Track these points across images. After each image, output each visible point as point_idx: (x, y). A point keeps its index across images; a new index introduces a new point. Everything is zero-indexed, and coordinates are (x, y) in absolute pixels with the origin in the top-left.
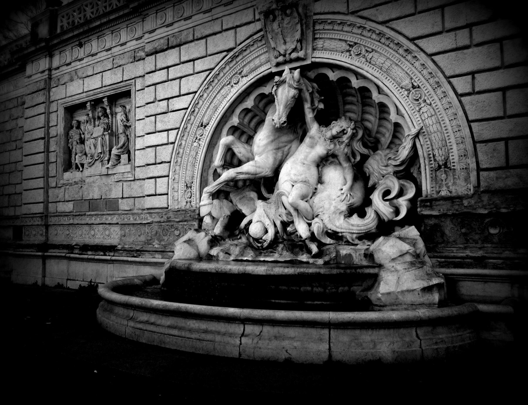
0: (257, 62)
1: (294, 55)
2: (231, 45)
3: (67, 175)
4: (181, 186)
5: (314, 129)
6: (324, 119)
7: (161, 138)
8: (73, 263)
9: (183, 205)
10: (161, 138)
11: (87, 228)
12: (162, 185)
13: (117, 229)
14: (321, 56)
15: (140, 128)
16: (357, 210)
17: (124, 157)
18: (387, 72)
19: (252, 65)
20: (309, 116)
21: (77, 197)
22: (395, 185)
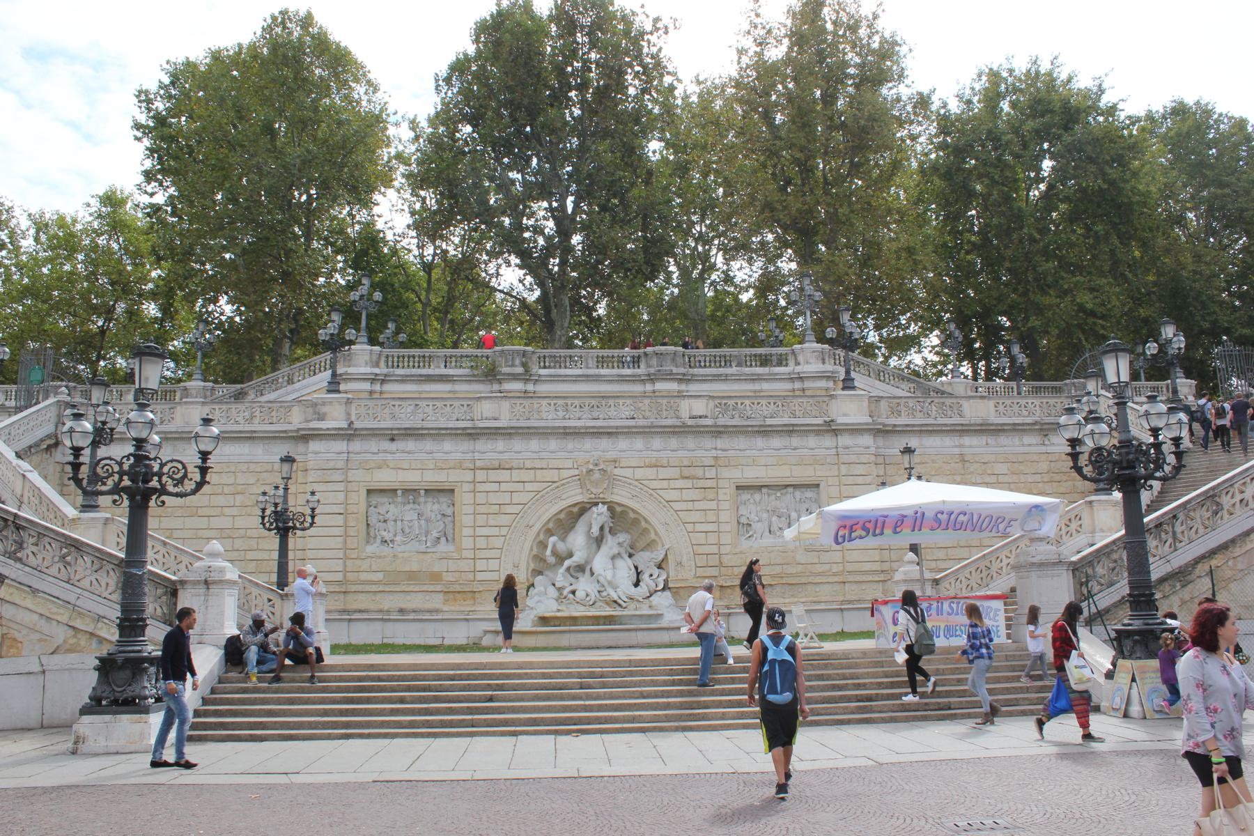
3: (370, 549)
5: (609, 537)
6: (612, 532)
7: (495, 531)
8: (390, 624)
10: (495, 531)
12: (493, 565)
13: (441, 595)
15: (467, 520)
16: (637, 585)
17: (443, 539)
20: (607, 530)
22: (656, 572)
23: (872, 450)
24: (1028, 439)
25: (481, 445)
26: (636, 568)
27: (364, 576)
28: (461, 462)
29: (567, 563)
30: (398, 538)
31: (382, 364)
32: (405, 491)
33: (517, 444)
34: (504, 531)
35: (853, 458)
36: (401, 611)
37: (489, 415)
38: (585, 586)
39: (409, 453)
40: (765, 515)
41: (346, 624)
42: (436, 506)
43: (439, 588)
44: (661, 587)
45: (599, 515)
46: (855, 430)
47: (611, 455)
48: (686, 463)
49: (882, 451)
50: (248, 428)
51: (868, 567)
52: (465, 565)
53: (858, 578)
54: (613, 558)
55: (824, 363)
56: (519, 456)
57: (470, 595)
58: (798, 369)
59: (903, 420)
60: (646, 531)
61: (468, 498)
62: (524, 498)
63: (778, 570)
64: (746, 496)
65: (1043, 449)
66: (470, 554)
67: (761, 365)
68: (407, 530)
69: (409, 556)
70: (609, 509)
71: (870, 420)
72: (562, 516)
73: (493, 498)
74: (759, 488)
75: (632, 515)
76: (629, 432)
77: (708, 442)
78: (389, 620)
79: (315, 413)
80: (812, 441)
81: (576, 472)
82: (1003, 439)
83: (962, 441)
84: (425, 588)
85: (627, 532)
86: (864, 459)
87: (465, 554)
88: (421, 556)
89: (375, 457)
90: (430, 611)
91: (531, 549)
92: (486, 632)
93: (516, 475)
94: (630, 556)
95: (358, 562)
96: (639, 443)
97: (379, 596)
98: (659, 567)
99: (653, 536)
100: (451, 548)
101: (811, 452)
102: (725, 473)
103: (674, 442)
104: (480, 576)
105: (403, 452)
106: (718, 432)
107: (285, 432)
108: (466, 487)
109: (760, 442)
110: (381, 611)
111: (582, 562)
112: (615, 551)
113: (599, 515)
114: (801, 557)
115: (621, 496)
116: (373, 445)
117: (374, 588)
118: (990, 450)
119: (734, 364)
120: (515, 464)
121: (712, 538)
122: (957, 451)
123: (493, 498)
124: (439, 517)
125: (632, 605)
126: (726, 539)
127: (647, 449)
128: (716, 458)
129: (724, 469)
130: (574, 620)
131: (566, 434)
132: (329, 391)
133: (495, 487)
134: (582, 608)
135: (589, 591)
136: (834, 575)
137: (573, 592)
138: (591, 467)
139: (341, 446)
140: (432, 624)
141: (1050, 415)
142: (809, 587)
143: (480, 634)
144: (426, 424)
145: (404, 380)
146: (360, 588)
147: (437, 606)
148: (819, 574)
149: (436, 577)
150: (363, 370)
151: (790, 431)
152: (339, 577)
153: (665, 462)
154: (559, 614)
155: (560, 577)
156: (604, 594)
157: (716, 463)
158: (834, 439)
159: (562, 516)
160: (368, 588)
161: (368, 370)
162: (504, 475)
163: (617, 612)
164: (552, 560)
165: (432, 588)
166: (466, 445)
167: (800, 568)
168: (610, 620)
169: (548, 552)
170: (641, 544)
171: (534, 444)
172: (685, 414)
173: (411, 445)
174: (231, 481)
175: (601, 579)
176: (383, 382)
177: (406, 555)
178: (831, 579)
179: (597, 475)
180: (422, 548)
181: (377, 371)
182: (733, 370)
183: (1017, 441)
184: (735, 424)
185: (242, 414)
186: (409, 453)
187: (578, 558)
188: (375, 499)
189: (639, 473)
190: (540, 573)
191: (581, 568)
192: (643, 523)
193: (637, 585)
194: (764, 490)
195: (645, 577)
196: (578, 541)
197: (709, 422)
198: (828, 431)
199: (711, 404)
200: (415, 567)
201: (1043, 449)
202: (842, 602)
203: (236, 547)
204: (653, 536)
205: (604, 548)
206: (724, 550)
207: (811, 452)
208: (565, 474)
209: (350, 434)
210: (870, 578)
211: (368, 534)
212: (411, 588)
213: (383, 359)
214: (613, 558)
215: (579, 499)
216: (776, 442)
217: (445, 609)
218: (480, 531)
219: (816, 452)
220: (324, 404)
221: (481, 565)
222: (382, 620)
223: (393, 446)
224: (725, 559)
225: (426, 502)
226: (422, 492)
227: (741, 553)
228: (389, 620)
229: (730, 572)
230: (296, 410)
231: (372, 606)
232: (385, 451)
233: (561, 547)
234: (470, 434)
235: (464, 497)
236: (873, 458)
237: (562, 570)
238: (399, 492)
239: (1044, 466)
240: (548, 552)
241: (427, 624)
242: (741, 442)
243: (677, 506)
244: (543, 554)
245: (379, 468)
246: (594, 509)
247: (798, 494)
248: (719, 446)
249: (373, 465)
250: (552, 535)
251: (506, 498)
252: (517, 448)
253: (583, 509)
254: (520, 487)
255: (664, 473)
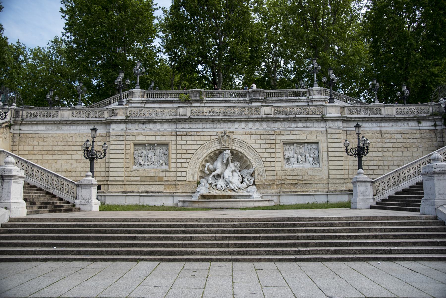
0: (216, 145)
1: (228, 146)
2: (209, 140)
3: (135, 167)
4: (190, 174)
5: (231, 163)
9: (191, 180)
11: (147, 186)
13: (163, 186)
14: (234, 148)
15: (173, 156)
16: (242, 183)
17: (164, 164)
18: (249, 154)
19: (215, 146)
20: (230, 160)
21: (142, 175)
22: (250, 178)
23: (341, 128)
24: (411, 124)
25: (179, 126)
26: (242, 176)
27: (132, 178)
28: (171, 133)
29: (213, 173)
30: (146, 163)
31: (145, 96)
32: (149, 144)
33: (194, 125)
34: (188, 160)
35: (333, 132)
36: (147, 192)
37: (182, 114)
38: (221, 183)
39: (150, 129)
40: (295, 155)
41: (125, 197)
42: (161, 151)
43: (162, 183)
44: (252, 184)
45: (227, 154)
46: (334, 120)
47: (231, 130)
48: (262, 133)
49: (345, 129)
50: (87, 119)
51: (339, 177)
52: (173, 174)
53: (334, 182)
54: (232, 172)
55: (321, 95)
56: (194, 130)
57: (174, 186)
58: (310, 97)
59: (355, 116)
60: (246, 161)
61: (174, 147)
62: (196, 147)
63: (300, 177)
64: (287, 147)
65: (418, 128)
66: (174, 170)
67: (295, 96)
68: (150, 160)
69: (151, 170)
70: (231, 152)
71: (341, 116)
72: (212, 154)
73: (184, 147)
74: (293, 144)
75: (240, 155)
76: (239, 120)
77: (272, 125)
78: (142, 196)
79: (113, 113)
80: (315, 124)
81: (217, 137)
82: (399, 124)
83: (381, 125)
84: (156, 183)
85: (239, 162)
86: (337, 132)
87: (173, 170)
88: (155, 170)
89: (137, 131)
90: (158, 192)
91: (199, 168)
92: (180, 201)
93: (193, 138)
94: (240, 171)
95: (130, 173)
96: (243, 125)
97: (138, 186)
98: (251, 176)
99: (249, 163)
100: (167, 167)
101: (315, 129)
102: (279, 137)
103: (257, 125)
104: (178, 179)
105: (148, 129)
106: (276, 120)
107: (101, 121)
108: (173, 143)
109: (293, 125)
110: (139, 192)
111: (219, 173)
112: (233, 168)
113: (227, 154)
114: (310, 173)
115: (236, 147)
116: (136, 126)
117: (136, 183)
118: (393, 128)
119: (284, 96)
120: (193, 134)
121: (273, 164)
122: (378, 129)
123: (184, 147)
124: (163, 155)
125: (240, 191)
126: (279, 164)
127: (247, 128)
128: (274, 131)
129: (278, 136)
130: (215, 197)
131: (213, 121)
132: (119, 105)
133: (185, 143)
134: (219, 192)
135: (222, 185)
136: (324, 180)
137: (216, 185)
138: (223, 134)
139: (123, 126)
140: (159, 198)
141: (421, 113)
142: (313, 185)
143: (177, 202)
144: (157, 118)
145: (154, 102)
146: (130, 183)
147: (161, 190)
148: (319, 179)
149: (161, 179)
150: (138, 99)
151: (306, 120)
152: (122, 178)
153: (254, 133)
154: (209, 194)
155: (211, 180)
156: (228, 186)
157: (276, 133)
158: (325, 123)
159: (212, 154)
160: (134, 183)
161: (140, 99)
162: (188, 138)
163: (233, 194)
164: (207, 172)
165: (159, 183)
166: (173, 126)
167: (310, 177)
168: (230, 197)
169: (206, 169)
170: (244, 166)
171: (201, 125)
172: (262, 112)
173: (151, 126)
174: (80, 140)
175: (227, 180)
176: (146, 103)
177: (149, 170)
178: (323, 182)
179: (226, 138)
180: (155, 167)
181: (143, 99)
182: (284, 98)
183: (406, 124)
184: (282, 117)
185: (85, 114)
186: (150, 129)
187: (218, 172)
188: (137, 148)
189: (243, 137)
190: (203, 178)
191: (219, 176)
192: (245, 158)
193: (242, 183)
194: (295, 145)
195: (246, 179)
196: (219, 165)
197: (272, 116)
198: (322, 120)
199: (273, 109)
200: (152, 175)
201: (418, 128)
202: (328, 192)
203: (82, 166)
204: (249, 163)
205: (228, 168)
206: (277, 169)
207: (315, 129)
208: (213, 137)
209: (127, 121)
210: (340, 182)
211: (134, 161)
212: (151, 183)
213: (146, 94)
214: (232, 172)
215: (218, 148)
216: (301, 125)
217: (164, 192)
218: (178, 161)
219: (317, 129)
220: (116, 109)
221: (179, 174)
222: (139, 196)
223: (144, 126)
224: (279, 173)
225: (157, 149)
226: (156, 145)
227: (285, 170)
228: (142, 196)
229: (281, 178)
230: (106, 112)
231: (135, 190)
232: (141, 129)
233: (211, 167)
234: (174, 122)
235: (172, 147)
236: (341, 131)
237: (211, 176)
238: (147, 145)
239: (418, 135)
240: (206, 169)
241: (157, 197)
242: (286, 125)
243: (259, 151)
244: (204, 170)
245: (139, 135)
246: (225, 152)
247: (309, 146)
248: (276, 127)
249: (136, 134)
250: (208, 162)
251: (189, 147)
252: (194, 127)
253: (221, 152)
254: (195, 143)
255: (253, 137)
